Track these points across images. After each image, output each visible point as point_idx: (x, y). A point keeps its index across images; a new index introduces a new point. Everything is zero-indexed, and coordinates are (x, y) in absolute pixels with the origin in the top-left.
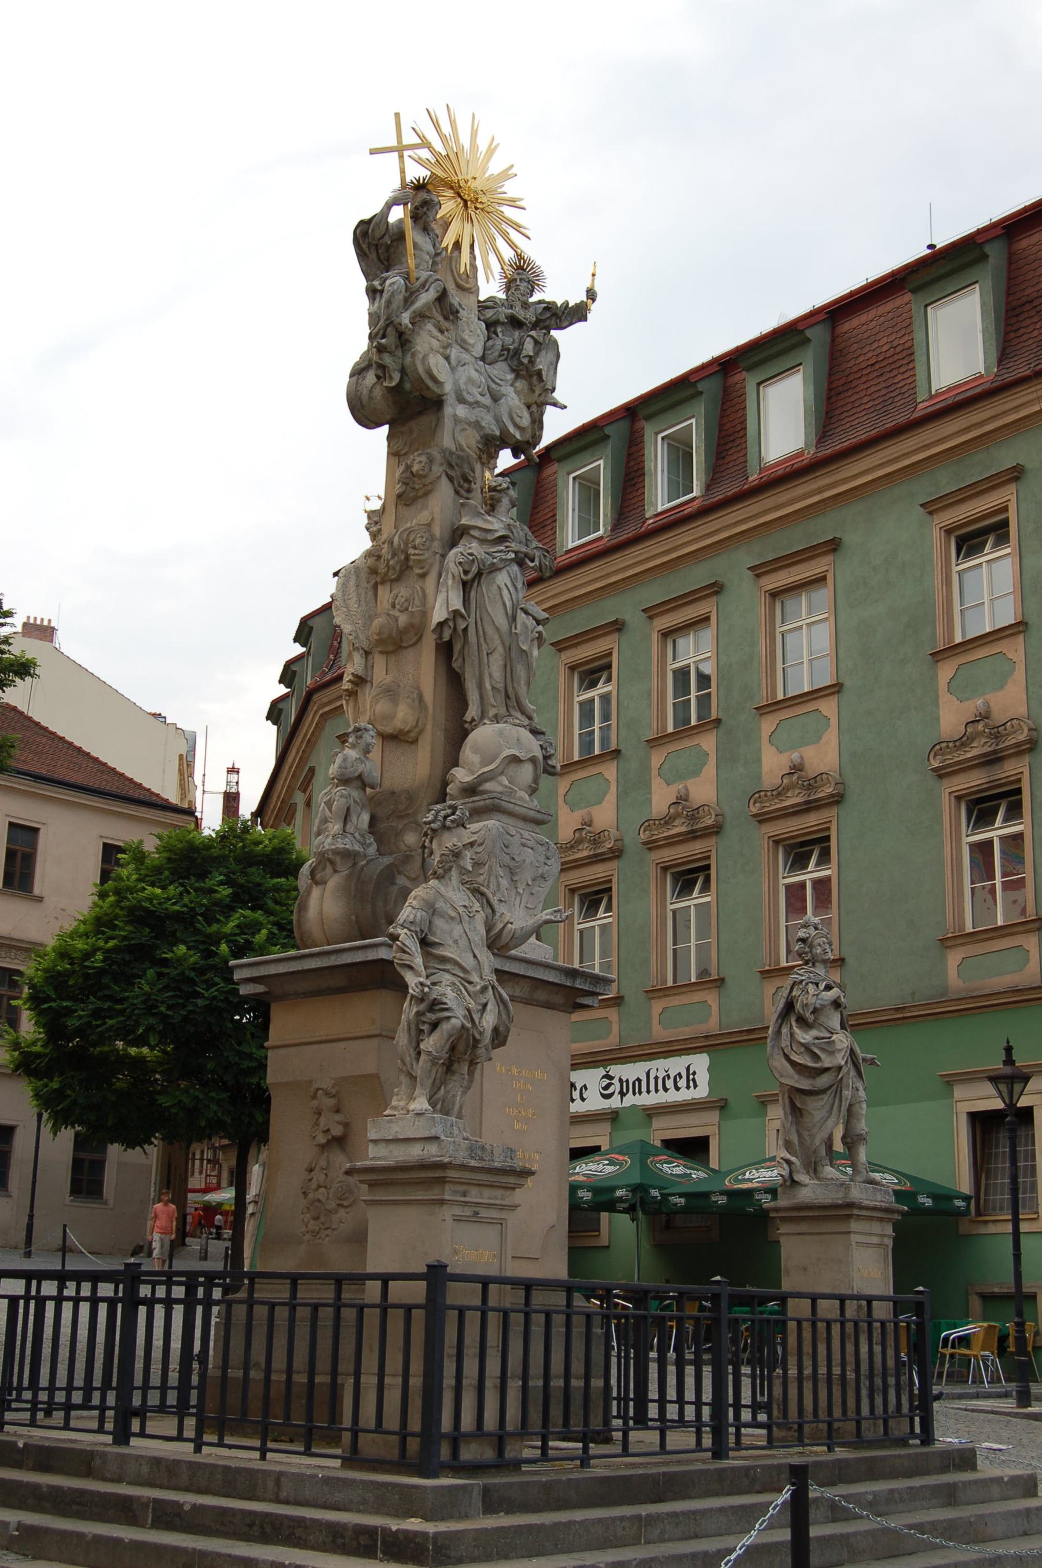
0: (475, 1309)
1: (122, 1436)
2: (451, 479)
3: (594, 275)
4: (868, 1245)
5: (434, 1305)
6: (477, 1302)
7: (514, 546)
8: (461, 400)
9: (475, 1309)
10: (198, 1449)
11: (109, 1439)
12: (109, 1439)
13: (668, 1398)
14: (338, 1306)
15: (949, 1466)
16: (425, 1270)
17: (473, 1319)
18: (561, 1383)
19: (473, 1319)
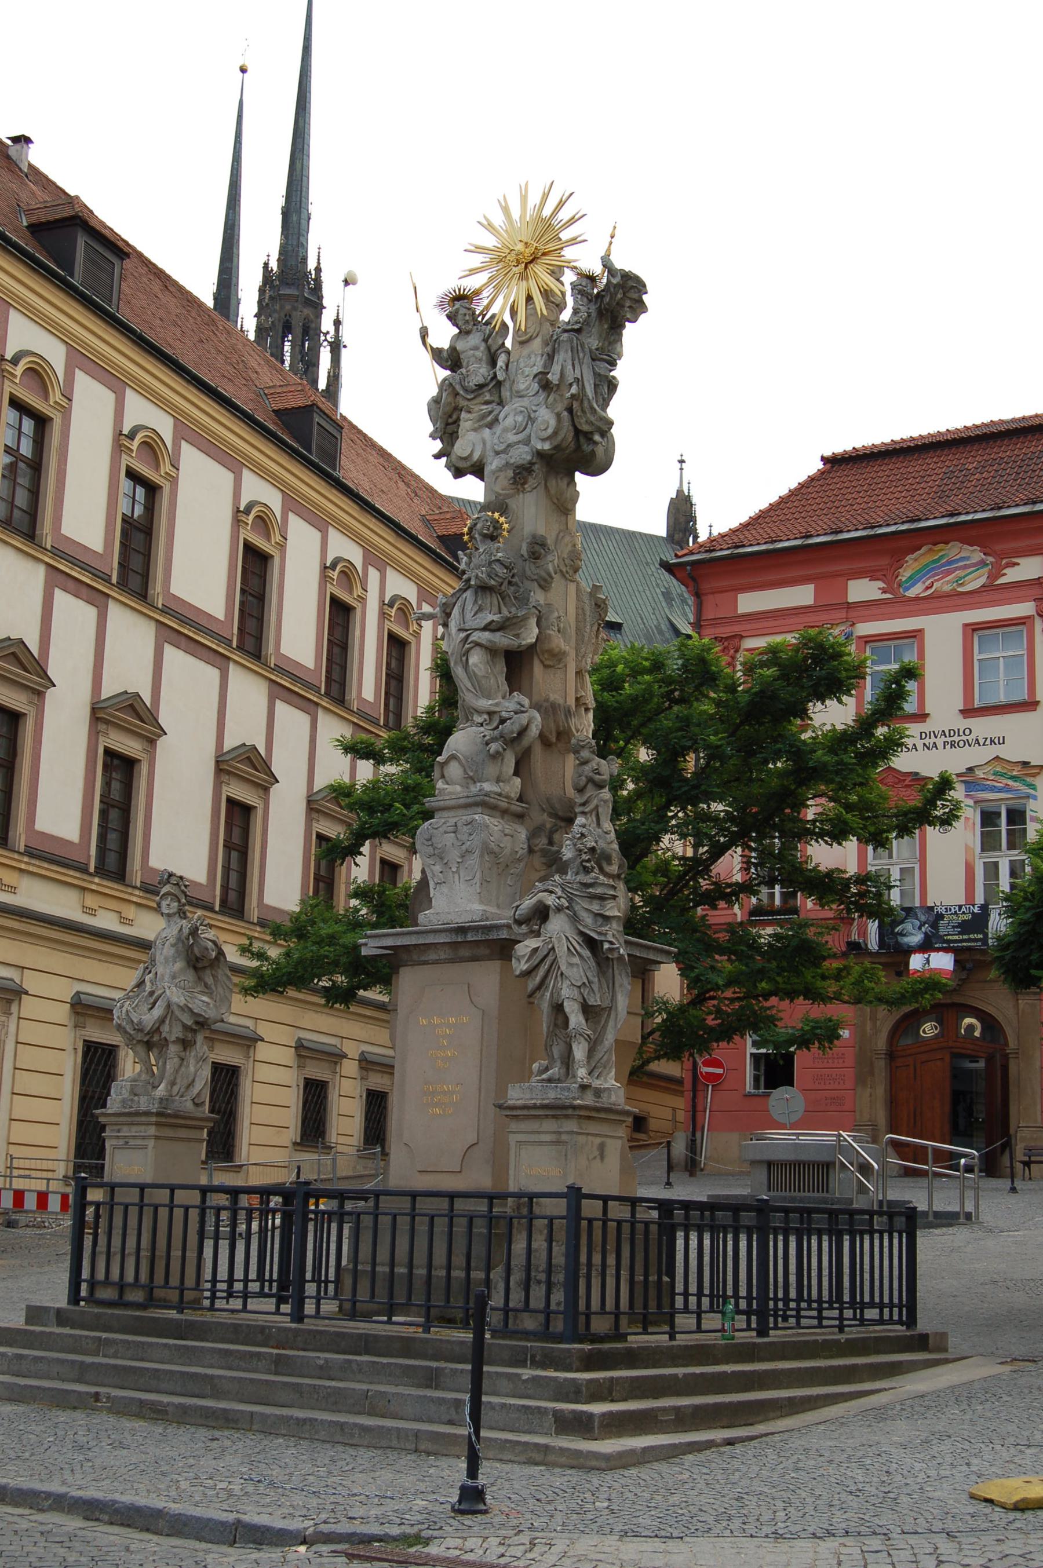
0: (165, 1206)
1: (762, 1332)
3: (612, 237)
4: (541, 1143)
5: (575, 1214)
6: (136, 1200)
9: (165, 1206)
10: (672, 1337)
11: (754, 1333)
12: (754, 1333)
13: (695, 1298)
14: (111, 1205)
15: (525, 1361)
16: (566, 1190)
17: (133, 1211)
18: (443, 1273)
19: (133, 1211)
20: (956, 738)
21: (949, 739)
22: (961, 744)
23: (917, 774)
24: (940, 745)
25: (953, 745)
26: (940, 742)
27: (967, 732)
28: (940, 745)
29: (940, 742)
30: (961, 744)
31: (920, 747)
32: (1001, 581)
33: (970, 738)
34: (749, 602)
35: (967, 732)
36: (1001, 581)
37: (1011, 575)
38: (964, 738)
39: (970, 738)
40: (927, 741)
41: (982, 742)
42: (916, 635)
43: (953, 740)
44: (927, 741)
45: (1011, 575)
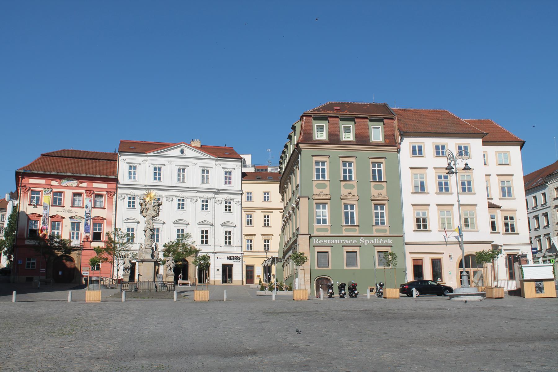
20: (69, 211)
29: (66, 211)
31: (63, 212)
32: (79, 186)
34: (32, 181)
36: (79, 186)
37: (81, 185)
40: (64, 211)
42: (62, 192)
44: (64, 211)
45: (81, 185)
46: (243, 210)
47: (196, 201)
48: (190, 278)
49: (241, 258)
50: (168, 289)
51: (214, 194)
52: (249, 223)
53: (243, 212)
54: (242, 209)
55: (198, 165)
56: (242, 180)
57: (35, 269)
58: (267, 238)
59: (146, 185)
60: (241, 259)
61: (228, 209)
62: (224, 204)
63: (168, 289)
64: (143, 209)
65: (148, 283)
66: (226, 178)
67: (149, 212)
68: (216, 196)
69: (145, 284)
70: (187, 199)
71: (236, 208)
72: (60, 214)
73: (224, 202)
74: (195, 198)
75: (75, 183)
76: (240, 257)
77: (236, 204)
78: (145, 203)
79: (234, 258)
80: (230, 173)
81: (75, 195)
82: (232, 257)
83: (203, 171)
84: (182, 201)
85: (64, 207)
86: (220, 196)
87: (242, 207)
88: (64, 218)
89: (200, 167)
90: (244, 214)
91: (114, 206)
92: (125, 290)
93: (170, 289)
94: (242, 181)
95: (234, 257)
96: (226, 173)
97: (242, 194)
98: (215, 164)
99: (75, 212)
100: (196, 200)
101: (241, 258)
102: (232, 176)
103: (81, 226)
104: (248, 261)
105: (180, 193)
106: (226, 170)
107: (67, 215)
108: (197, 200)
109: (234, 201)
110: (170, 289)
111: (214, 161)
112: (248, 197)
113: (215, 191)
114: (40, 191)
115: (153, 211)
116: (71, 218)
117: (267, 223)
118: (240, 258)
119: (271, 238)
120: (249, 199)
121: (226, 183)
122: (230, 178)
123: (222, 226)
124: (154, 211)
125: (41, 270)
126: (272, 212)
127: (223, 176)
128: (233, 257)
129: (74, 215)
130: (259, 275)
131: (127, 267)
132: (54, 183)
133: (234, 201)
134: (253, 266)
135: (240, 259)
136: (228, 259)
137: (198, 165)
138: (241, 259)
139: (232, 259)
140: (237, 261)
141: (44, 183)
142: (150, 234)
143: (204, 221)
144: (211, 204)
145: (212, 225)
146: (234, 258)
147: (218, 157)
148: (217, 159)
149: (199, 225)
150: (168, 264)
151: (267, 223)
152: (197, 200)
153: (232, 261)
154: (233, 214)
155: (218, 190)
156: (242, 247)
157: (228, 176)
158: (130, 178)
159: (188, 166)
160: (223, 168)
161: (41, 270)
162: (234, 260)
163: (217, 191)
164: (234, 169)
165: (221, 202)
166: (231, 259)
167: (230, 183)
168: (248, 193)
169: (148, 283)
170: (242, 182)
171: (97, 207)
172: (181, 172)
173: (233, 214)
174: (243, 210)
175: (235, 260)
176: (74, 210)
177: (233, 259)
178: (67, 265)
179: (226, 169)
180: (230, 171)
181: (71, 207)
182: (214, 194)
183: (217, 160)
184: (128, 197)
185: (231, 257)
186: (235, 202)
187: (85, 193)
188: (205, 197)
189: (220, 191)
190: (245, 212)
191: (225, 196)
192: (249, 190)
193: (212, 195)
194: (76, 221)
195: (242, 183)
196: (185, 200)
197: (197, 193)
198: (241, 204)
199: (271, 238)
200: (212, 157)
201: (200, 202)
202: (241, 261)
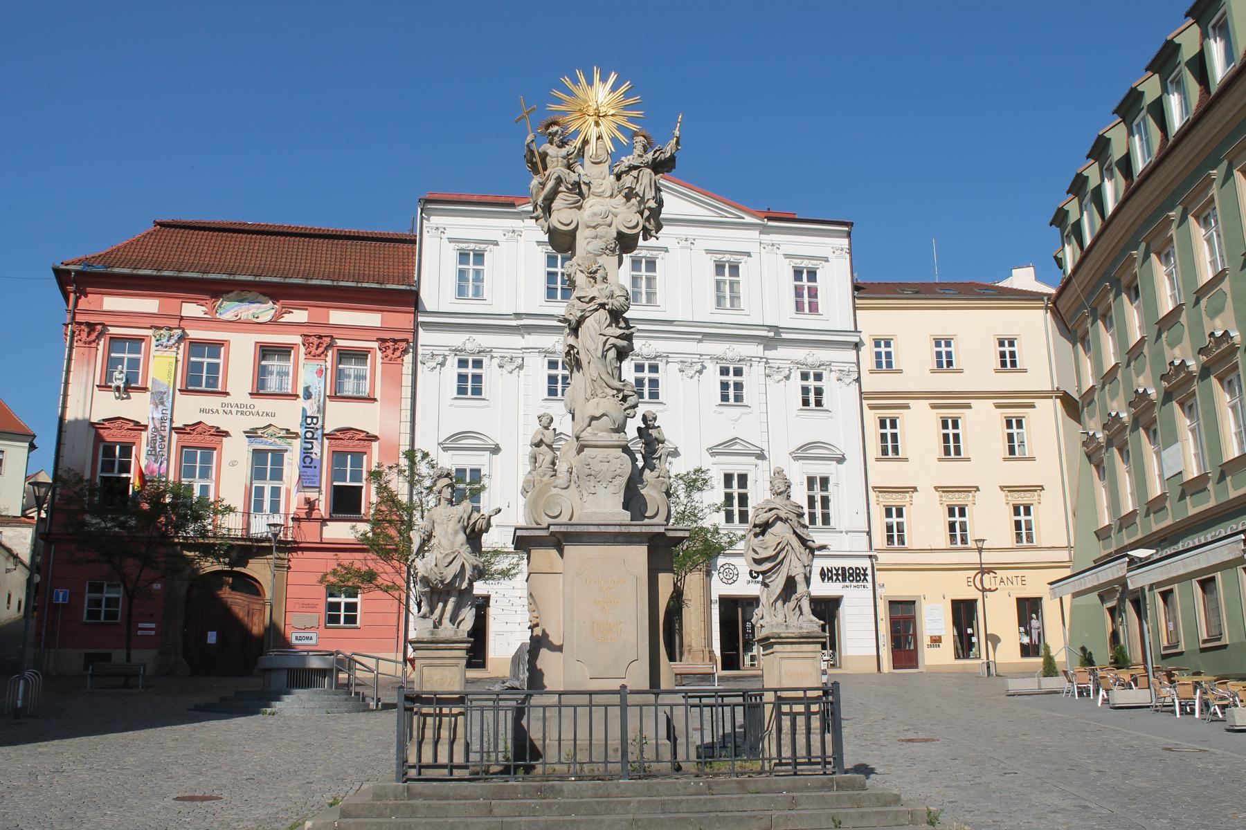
2: (581, 271)
7: (598, 301)
8: (588, 227)
20: (245, 410)
21: (240, 410)
22: (248, 413)
23: (218, 428)
24: (234, 412)
25: (242, 413)
26: (234, 410)
27: (252, 407)
28: (234, 412)
29: (234, 410)
30: (248, 413)
32: (280, 320)
33: (253, 410)
34: (112, 303)
35: (252, 407)
37: (287, 318)
38: (250, 410)
39: (253, 410)
40: (226, 409)
41: (261, 414)
42: (220, 344)
43: (242, 411)
44: (226, 409)
45: (287, 318)
46: (865, 402)
47: (700, 372)
48: (689, 651)
49: (869, 572)
50: (786, 752)
51: (761, 347)
52: (890, 447)
53: (865, 408)
54: (861, 400)
55: (701, 245)
56: (854, 297)
57: (117, 623)
58: (957, 500)
59: (518, 316)
60: (869, 578)
61: (813, 398)
62: (796, 383)
63: (786, 752)
64: (550, 184)
65: (624, 706)
66: (798, 292)
67: (593, 205)
68: (769, 354)
69: (598, 713)
70: (667, 362)
71: (839, 394)
72: (210, 420)
73: (796, 375)
74: (697, 360)
75: (265, 311)
76: (865, 570)
77: (839, 379)
78: (564, 151)
79: (844, 574)
80: (812, 275)
81: (266, 351)
82: (837, 570)
83: (719, 268)
84: (650, 371)
85: (227, 394)
86: (782, 352)
87: (861, 393)
88: (226, 434)
89: (708, 251)
90: (872, 418)
91: (407, 392)
92: (435, 766)
93: (801, 751)
94: (857, 301)
95: (843, 569)
96: (798, 274)
97: (857, 346)
98: (761, 243)
99: (267, 414)
100: (699, 367)
101: (869, 572)
102: (820, 283)
103: (288, 463)
104: (897, 586)
105: (644, 342)
106: (798, 263)
107: (236, 425)
108: (704, 367)
109: (833, 369)
110: (801, 751)
111: (755, 234)
112: (878, 355)
113: (765, 333)
114: (140, 340)
115: (620, 199)
116: (252, 434)
117: (952, 447)
118: (865, 575)
119: (971, 498)
120: (884, 363)
121: (799, 307)
122: (813, 293)
123: (796, 459)
124: (628, 197)
125: (140, 625)
126: (969, 407)
127: (789, 283)
128: (840, 572)
129: (261, 422)
130: (937, 634)
131: (449, 574)
132: (191, 309)
133: (831, 371)
134: (914, 602)
135: (865, 579)
136: (823, 580)
137: (701, 245)
138: (869, 578)
139: (837, 579)
140: (855, 584)
141: (156, 311)
142: (612, 340)
143: (734, 441)
144: (752, 379)
145: (761, 456)
146: (844, 574)
147: (770, 219)
148: (765, 226)
149: (713, 454)
150: (771, 552)
151: (952, 447)
152: (704, 367)
153: (839, 585)
154: (831, 417)
155: (775, 329)
156: (869, 533)
157: (805, 282)
158: (461, 292)
159: (667, 251)
160: (787, 256)
161: (140, 625)
162: (844, 580)
163: (772, 334)
164: (827, 260)
165: (787, 372)
166: (834, 578)
167: (814, 308)
168: (877, 344)
169: (624, 706)
170: (854, 302)
171: (346, 394)
172: (640, 270)
173: (830, 414)
174: (865, 402)
175: (848, 583)
176: (262, 404)
177: (840, 578)
178: (236, 609)
179: (798, 261)
180: (810, 266)
181: (250, 394)
182: (761, 347)
183: (764, 230)
184: (456, 357)
185: (834, 572)
186: (834, 375)
187: (301, 346)
188: (730, 355)
189: (784, 336)
190: (872, 407)
191: (800, 354)
192: (882, 333)
193: (755, 350)
194: (271, 444)
195: (855, 309)
196: (661, 366)
197: (700, 341)
198: (858, 380)
199: (971, 498)
200: (748, 219)
201: (713, 371)
202: (870, 585)
